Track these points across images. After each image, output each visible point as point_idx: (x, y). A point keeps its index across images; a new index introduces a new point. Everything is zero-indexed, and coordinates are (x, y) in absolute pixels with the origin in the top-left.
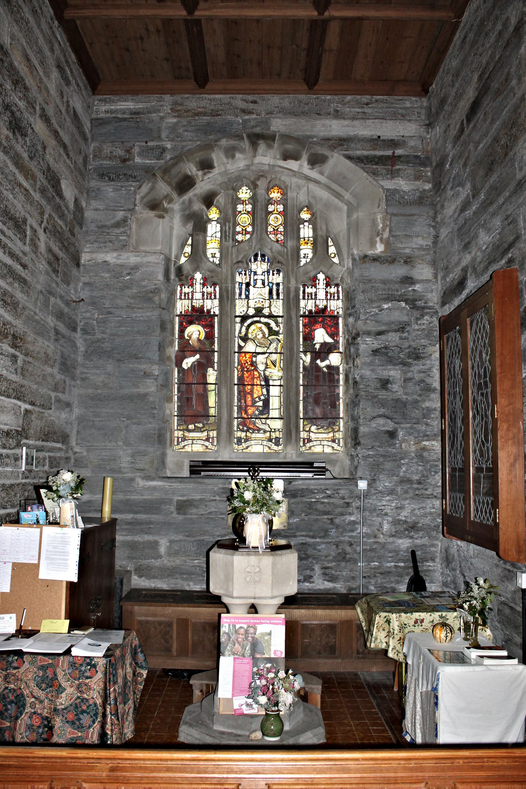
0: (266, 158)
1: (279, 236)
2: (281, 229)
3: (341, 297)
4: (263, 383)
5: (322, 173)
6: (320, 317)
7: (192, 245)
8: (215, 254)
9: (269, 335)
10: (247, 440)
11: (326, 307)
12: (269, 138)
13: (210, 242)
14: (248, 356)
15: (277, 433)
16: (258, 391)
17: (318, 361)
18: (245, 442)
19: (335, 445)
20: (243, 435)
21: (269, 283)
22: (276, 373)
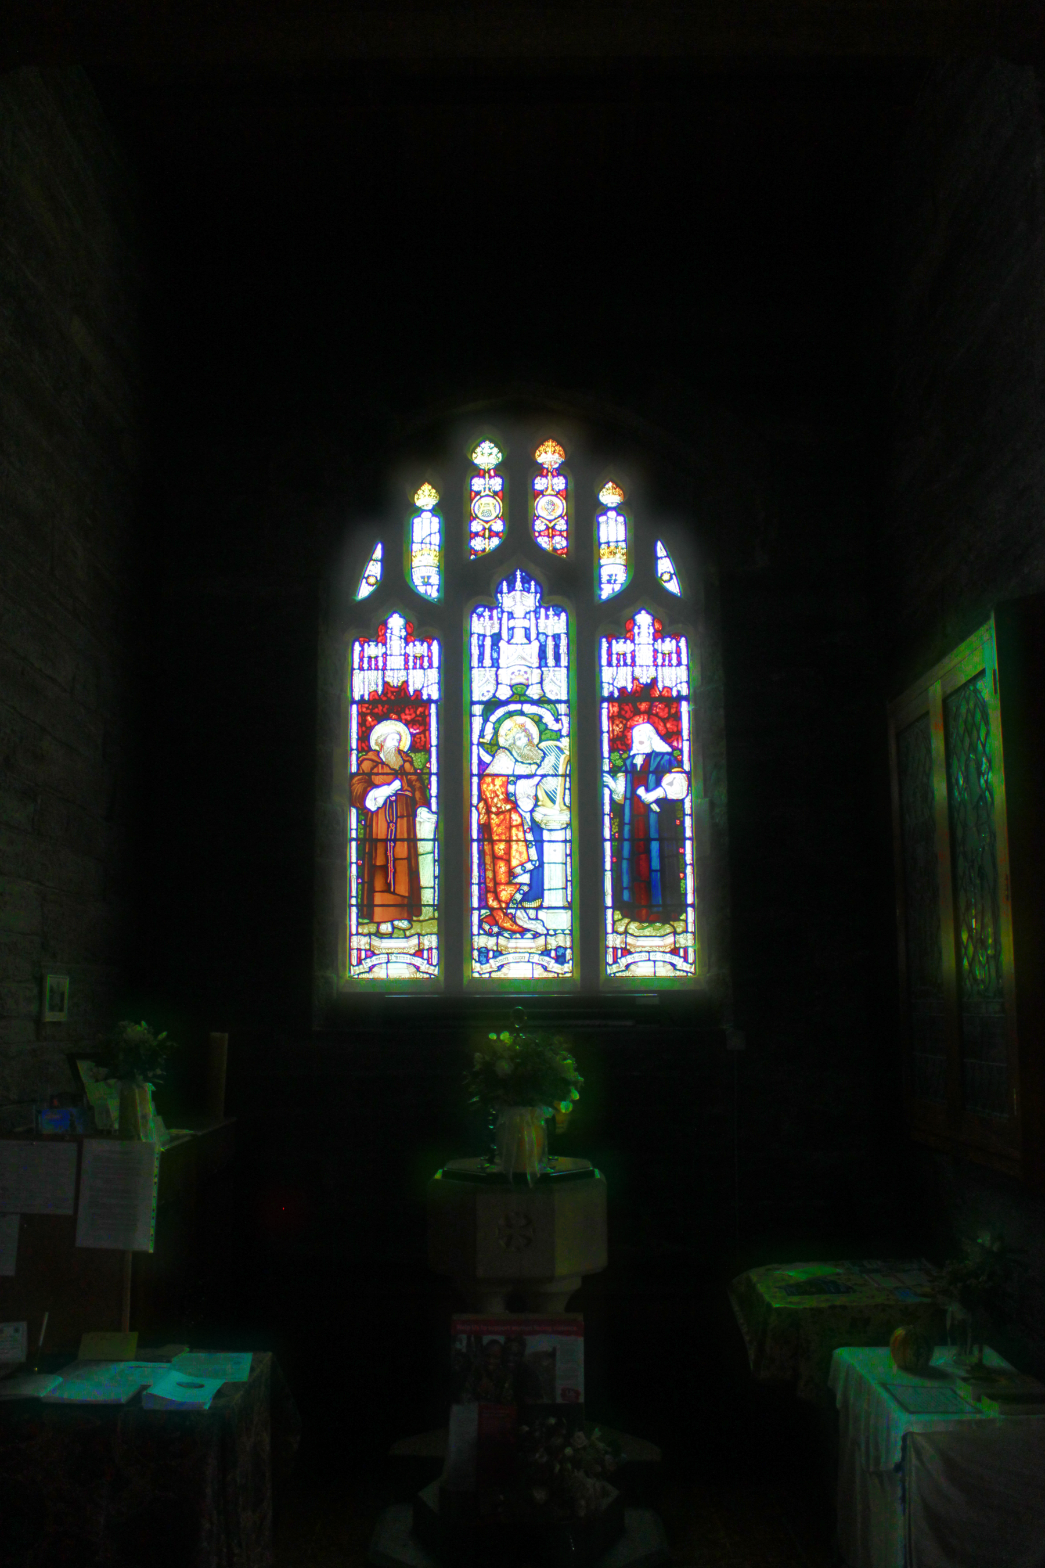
1: (557, 539)
2: (561, 525)
3: (684, 661)
4: (530, 837)
6: (644, 701)
7: (383, 561)
8: (429, 577)
9: (541, 741)
10: (498, 953)
11: (655, 681)
13: (419, 554)
14: (498, 781)
15: (561, 937)
16: (521, 853)
17: (641, 791)
18: (494, 957)
19: (678, 961)
20: (490, 942)
21: (538, 634)
22: (556, 817)
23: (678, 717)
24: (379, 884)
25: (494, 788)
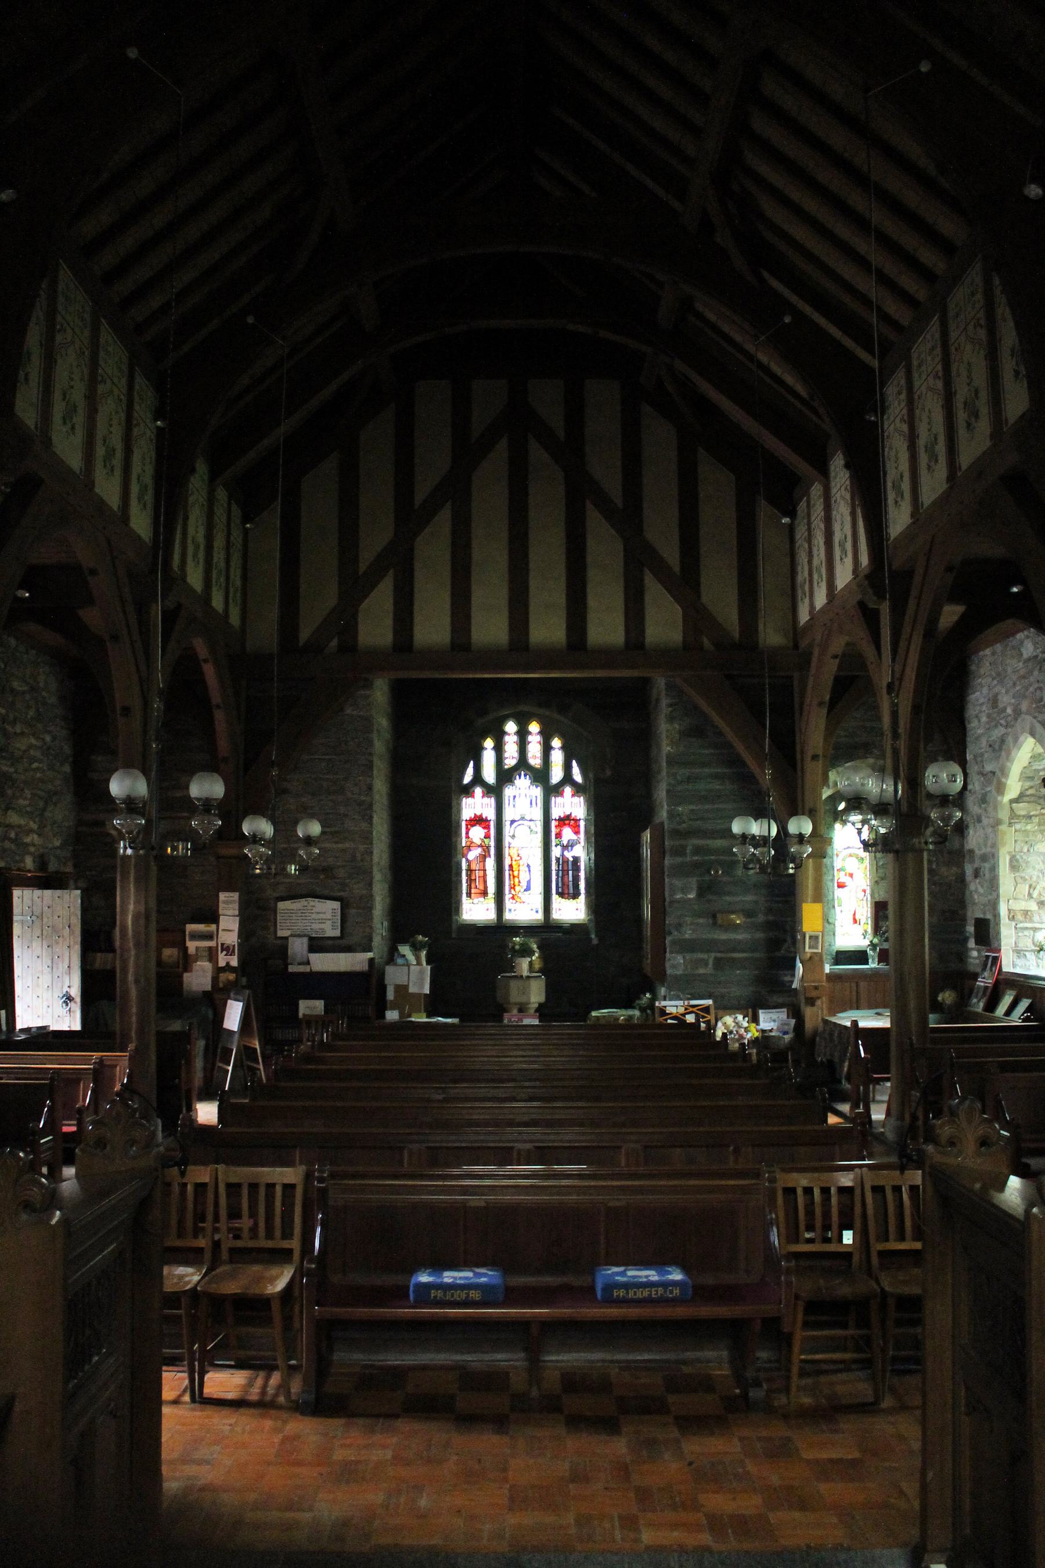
6: (566, 820)
17: (566, 853)
23: (579, 826)
24: (473, 886)
25: (514, 853)
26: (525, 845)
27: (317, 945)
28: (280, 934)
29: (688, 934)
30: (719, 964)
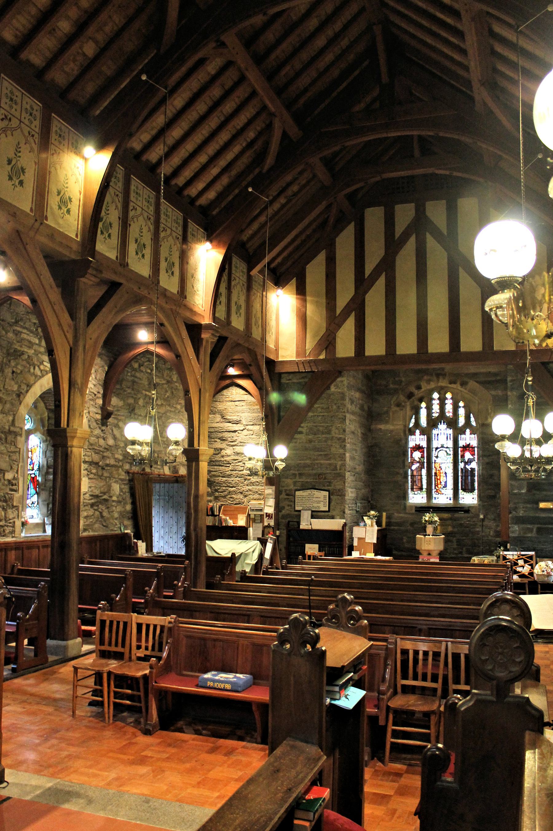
0: (443, 383)
5: (466, 389)
6: (467, 447)
12: (444, 375)
17: (467, 466)
25: (437, 465)
26: (444, 462)
27: (315, 515)
28: (297, 508)
29: (521, 513)
30: (539, 530)
